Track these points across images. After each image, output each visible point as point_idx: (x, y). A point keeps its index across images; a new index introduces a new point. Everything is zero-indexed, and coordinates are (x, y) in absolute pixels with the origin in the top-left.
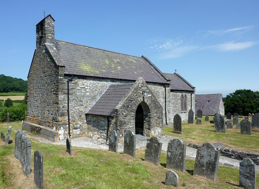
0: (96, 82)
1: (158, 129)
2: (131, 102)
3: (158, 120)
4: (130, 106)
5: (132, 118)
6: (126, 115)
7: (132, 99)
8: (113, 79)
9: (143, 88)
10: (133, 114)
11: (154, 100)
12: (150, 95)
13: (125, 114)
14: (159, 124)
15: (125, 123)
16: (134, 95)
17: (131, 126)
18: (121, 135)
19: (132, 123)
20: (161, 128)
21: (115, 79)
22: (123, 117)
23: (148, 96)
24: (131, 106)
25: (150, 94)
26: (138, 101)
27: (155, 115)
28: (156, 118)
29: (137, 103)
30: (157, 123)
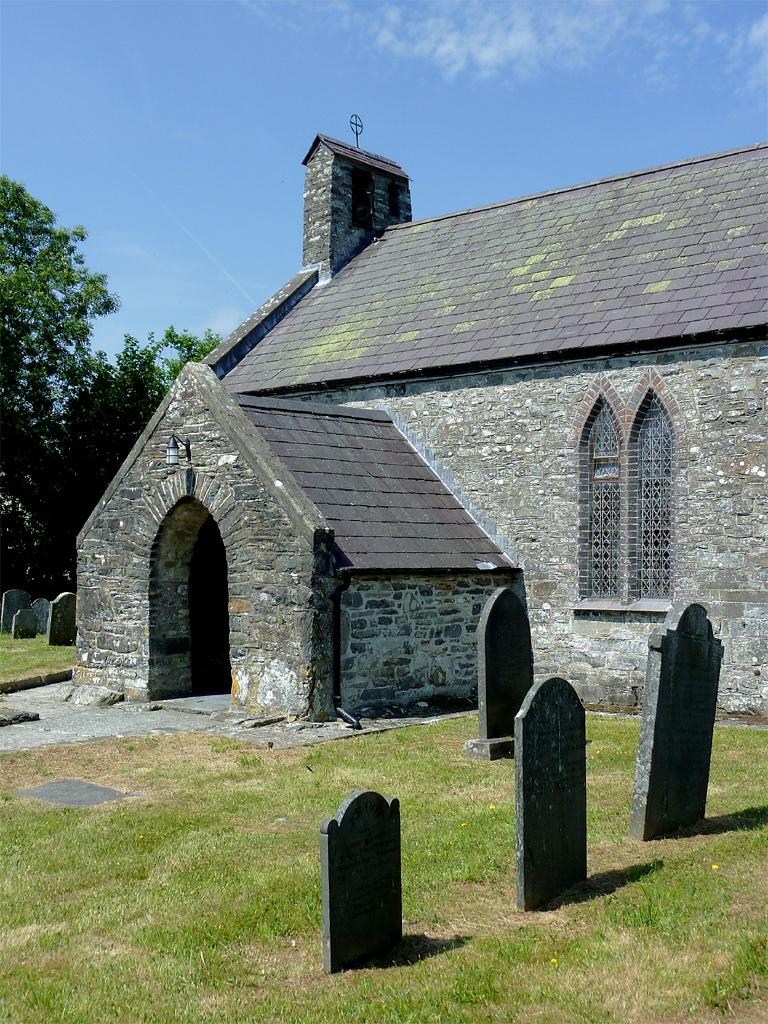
0: (473, 396)
1: (273, 671)
2: (130, 504)
3: (272, 613)
4: (121, 524)
5: (131, 580)
6: (106, 564)
7: (134, 485)
8: (397, 376)
9: (189, 424)
10: (135, 560)
11: (255, 487)
12: (231, 459)
13: (103, 561)
14: (284, 637)
15: (104, 600)
16: (144, 466)
17: (130, 624)
18: (85, 657)
19: (134, 609)
20: (291, 664)
21: (411, 374)
22: (95, 574)
23: (220, 463)
24: (126, 522)
25: (228, 452)
26: (163, 495)
27: (259, 577)
28: (264, 596)
29: (159, 506)
30: (264, 630)
